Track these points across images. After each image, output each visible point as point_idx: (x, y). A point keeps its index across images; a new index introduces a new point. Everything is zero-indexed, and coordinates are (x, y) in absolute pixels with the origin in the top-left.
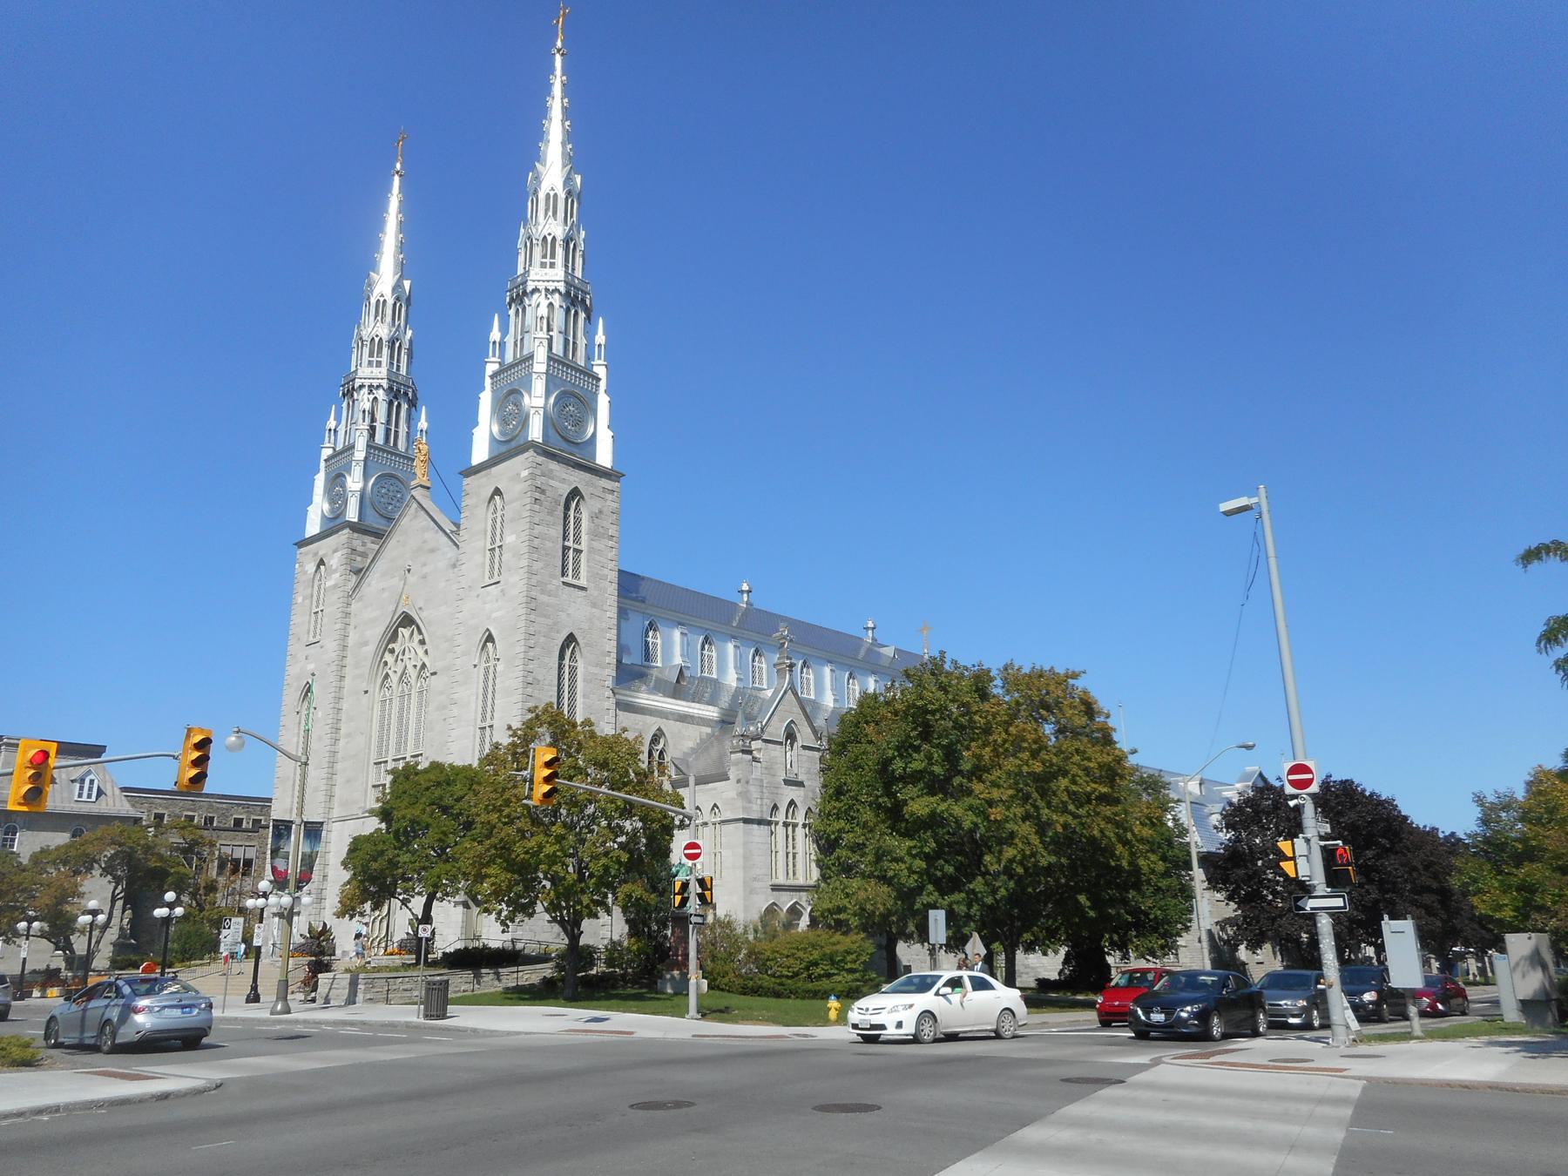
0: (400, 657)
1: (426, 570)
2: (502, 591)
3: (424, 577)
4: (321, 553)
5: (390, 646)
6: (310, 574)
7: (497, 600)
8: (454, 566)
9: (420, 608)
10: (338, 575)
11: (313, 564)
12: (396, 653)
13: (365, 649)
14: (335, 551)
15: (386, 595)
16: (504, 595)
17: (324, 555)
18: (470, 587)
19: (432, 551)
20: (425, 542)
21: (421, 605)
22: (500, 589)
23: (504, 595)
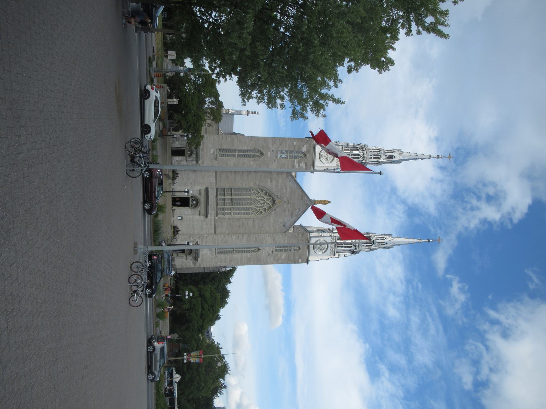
0: (263, 199)
1: (287, 211)
2: (270, 254)
3: (285, 211)
4: (308, 155)
5: (267, 194)
6: (302, 149)
7: (268, 252)
8: (284, 226)
9: (275, 210)
10: (297, 167)
11: (305, 150)
12: (264, 197)
13: (269, 180)
14: (306, 165)
15: (284, 190)
16: (268, 255)
17: (306, 158)
18: (275, 239)
19: (292, 214)
20: (296, 210)
21: (277, 210)
22: (271, 253)
23: (268, 255)
